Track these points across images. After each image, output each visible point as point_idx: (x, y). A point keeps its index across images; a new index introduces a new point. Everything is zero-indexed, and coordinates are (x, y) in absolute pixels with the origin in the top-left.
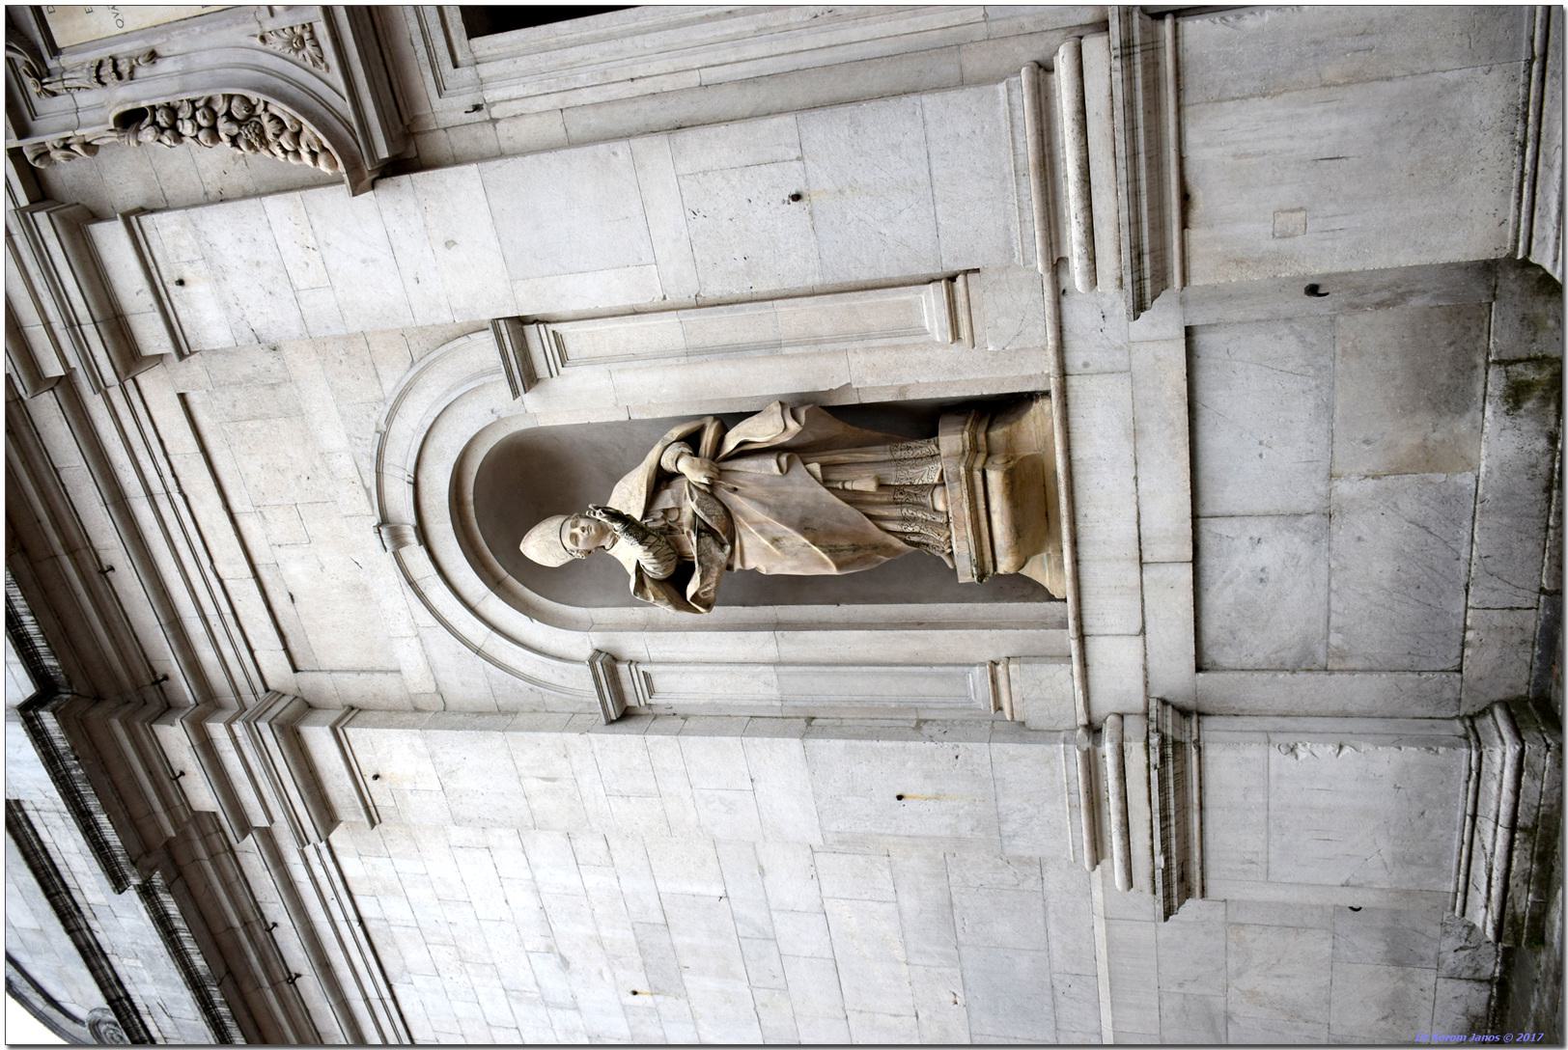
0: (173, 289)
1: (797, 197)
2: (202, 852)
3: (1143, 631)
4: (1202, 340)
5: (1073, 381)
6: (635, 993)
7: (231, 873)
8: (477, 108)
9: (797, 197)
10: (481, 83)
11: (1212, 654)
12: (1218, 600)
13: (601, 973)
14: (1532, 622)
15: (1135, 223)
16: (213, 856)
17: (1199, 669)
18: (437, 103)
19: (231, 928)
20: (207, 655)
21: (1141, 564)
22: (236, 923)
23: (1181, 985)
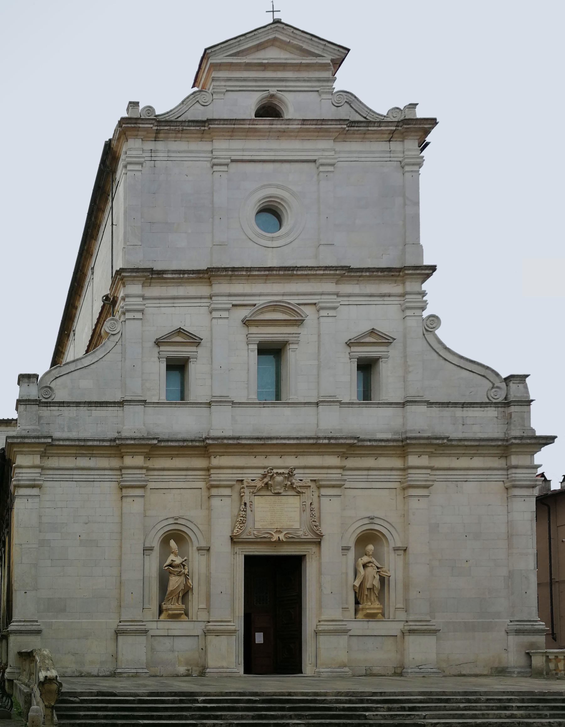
0: (221, 499)
1: (221, 592)
2: (112, 452)
3: (157, 629)
4: (197, 637)
5: (193, 622)
6: (80, 536)
7: (105, 455)
8: (236, 553)
9: (221, 592)
10: (239, 554)
11: (153, 638)
12: (161, 638)
13: (84, 530)
14: (158, 674)
15: (214, 630)
16: (111, 454)
17: (151, 636)
18: (238, 548)
19: (93, 450)
20: (156, 473)
21: (168, 629)
22: (94, 452)
23: (93, 632)
